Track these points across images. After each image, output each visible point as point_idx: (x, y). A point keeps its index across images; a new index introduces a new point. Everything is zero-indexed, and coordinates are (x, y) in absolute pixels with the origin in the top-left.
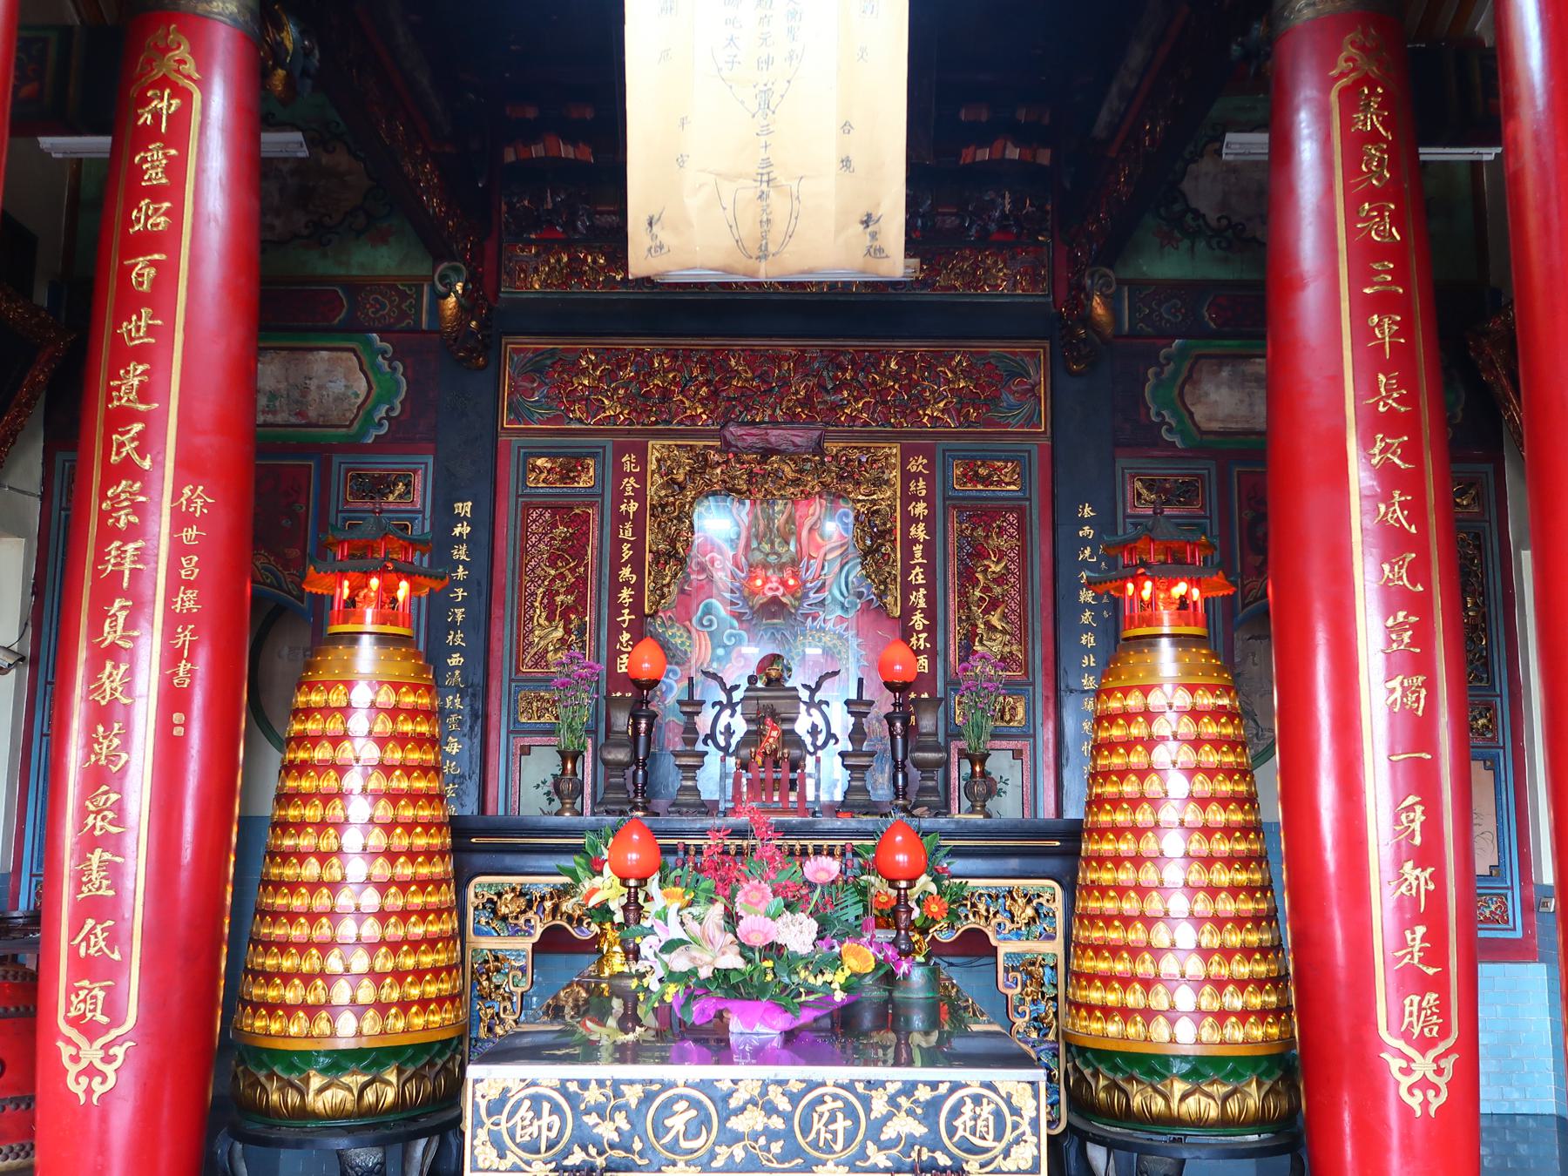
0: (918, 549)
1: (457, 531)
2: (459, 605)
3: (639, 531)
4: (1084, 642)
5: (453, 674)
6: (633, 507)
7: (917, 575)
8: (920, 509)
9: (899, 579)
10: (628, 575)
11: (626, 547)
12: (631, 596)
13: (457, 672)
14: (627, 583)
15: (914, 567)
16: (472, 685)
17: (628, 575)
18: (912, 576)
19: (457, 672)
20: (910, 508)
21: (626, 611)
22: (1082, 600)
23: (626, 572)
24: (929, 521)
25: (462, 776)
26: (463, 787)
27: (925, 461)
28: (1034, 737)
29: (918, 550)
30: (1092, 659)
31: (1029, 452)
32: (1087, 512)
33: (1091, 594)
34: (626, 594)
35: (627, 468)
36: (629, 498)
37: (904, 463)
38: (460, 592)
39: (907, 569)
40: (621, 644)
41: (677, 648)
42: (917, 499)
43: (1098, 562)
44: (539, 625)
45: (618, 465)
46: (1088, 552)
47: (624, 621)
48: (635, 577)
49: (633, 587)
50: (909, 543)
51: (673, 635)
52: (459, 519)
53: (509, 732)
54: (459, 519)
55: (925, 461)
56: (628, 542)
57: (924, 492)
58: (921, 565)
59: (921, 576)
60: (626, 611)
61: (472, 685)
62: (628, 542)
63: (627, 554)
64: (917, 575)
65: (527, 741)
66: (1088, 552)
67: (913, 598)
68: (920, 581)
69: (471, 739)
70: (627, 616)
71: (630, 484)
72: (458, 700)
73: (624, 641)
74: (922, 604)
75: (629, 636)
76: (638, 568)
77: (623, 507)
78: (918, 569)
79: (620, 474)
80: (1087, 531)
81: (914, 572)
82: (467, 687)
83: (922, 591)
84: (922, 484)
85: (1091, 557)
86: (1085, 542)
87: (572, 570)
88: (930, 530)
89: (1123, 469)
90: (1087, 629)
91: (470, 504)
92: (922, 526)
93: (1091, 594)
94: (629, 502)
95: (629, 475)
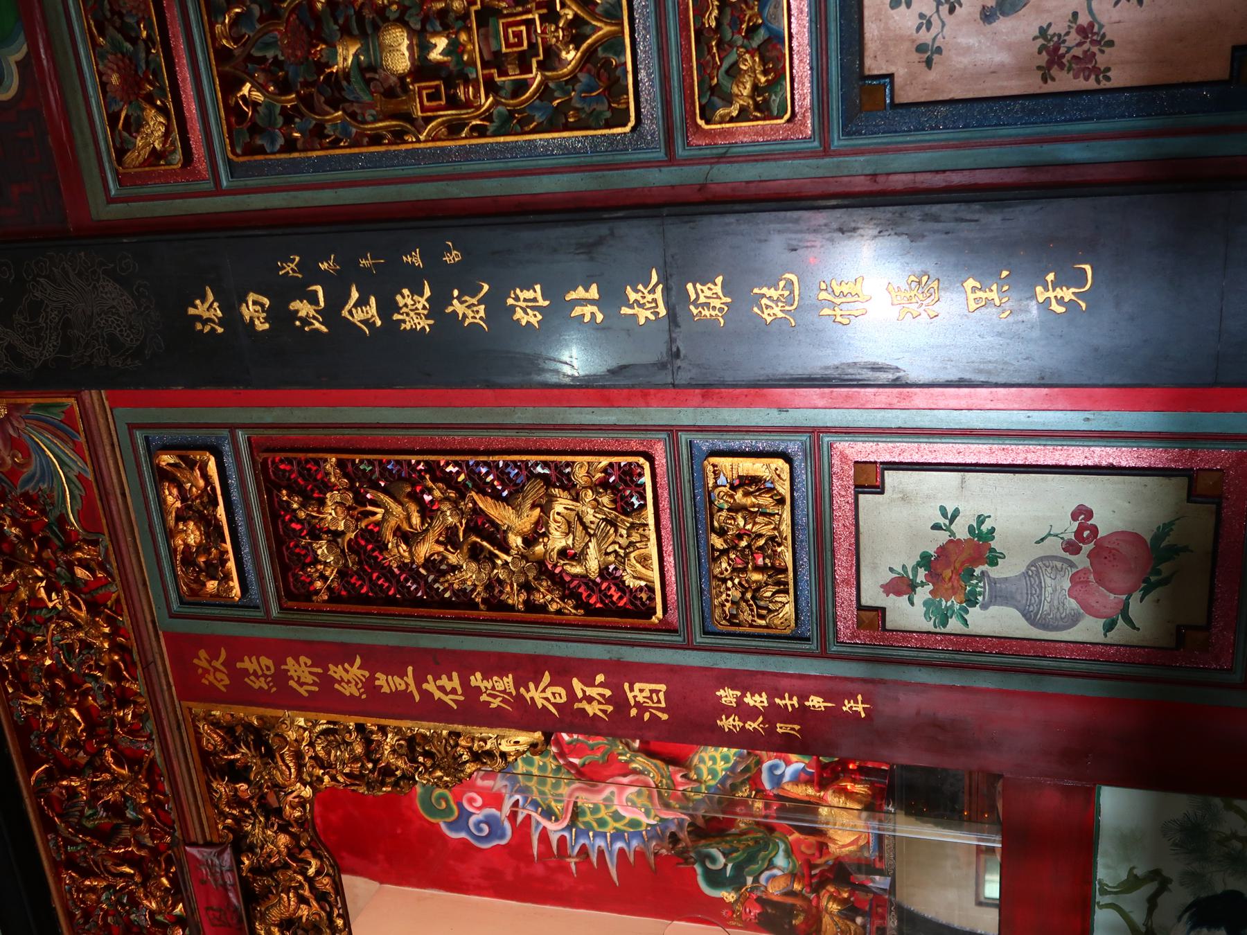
0: (387, 683)
4: (534, 318)
7: (442, 689)
8: (301, 671)
9: (459, 728)
15: (426, 695)
18: (447, 699)
20: (302, 691)
22: (424, 324)
24: (323, 655)
27: (203, 654)
28: (816, 432)
29: (387, 683)
30: (580, 293)
31: (132, 427)
32: (207, 309)
33: (405, 298)
37: (212, 696)
39: (432, 709)
41: (732, 769)
42: (281, 677)
43: (322, 278)
46: (303, 308)
50: (375, 702)
51: (713, 772)
55: (203, 654)
57: (265, 661)
58: (420, 680)
59: (444, 681)
64: (442, 689)
66: (303, 308)
67: (496, 703)
68: (456, 683)
74: (506, 684)
78: (430, 686)
80: (253, 309)
81: (438, 694)
83: (476, 680)
84: (248, 664)
85: (313, 300)
86: (280, 315)
88: (345, 654)
89: (111, 200)
90: (498, 309)
92: (336, 671)
93: (405, 298)
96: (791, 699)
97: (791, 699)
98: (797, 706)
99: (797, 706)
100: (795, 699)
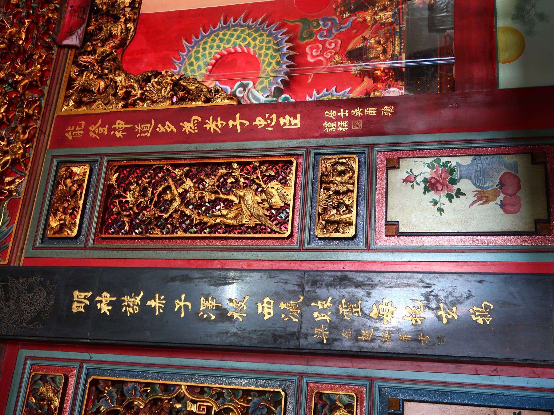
1: (105, 308)
2: (196, 305)
3: (145, 117)
5: (285, 311)
6: (121, 124)
10: (191, 125)
11: (161, 129)
12: (215, 119)
13: (283, 306)
14: (200, 125)
16: (301, 285)
17: (191, 125)
19: (283, 306)
21: (231, 123)
23: (188, 127)
25: (427, 297)
26: (442, 295)
34: (211, 125)
35: (79, 133)
36: (110, 130)
38: (180, 304)
40: (268, 125)
44: (235, 218)
45: (76, 143)
47: (242, 125)
48: (195, 117)
49: (205, 119)
52: (92, 308)
53: (368, 249)
54: (92, 308)
56: (156, 126)
60: (231, 123)
61: (301, 285)
62: (156, 126)
63: (170, 127)
65: (380, 226)
69: (373, 286)
70: (237, 123)
71: (96, 130)
72: (320, 304)
73: (264, 123)
75: (259, 118)
76: (187, 115)
77: (118, 135)
79: (86, 141)
82: (303, 292)
87: (179, 182)
91: (76, 293)
94: (115, 130)
95: (87, 130)
96: (344, 112)
97: (344, 112)
98: (347, 115)
99: (347, 115)
100: (347, 111)
